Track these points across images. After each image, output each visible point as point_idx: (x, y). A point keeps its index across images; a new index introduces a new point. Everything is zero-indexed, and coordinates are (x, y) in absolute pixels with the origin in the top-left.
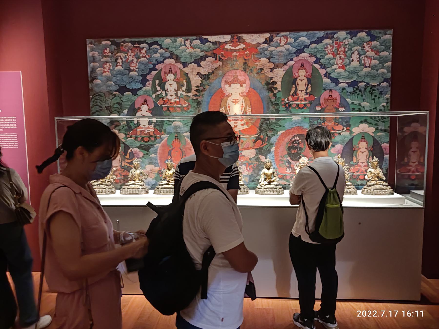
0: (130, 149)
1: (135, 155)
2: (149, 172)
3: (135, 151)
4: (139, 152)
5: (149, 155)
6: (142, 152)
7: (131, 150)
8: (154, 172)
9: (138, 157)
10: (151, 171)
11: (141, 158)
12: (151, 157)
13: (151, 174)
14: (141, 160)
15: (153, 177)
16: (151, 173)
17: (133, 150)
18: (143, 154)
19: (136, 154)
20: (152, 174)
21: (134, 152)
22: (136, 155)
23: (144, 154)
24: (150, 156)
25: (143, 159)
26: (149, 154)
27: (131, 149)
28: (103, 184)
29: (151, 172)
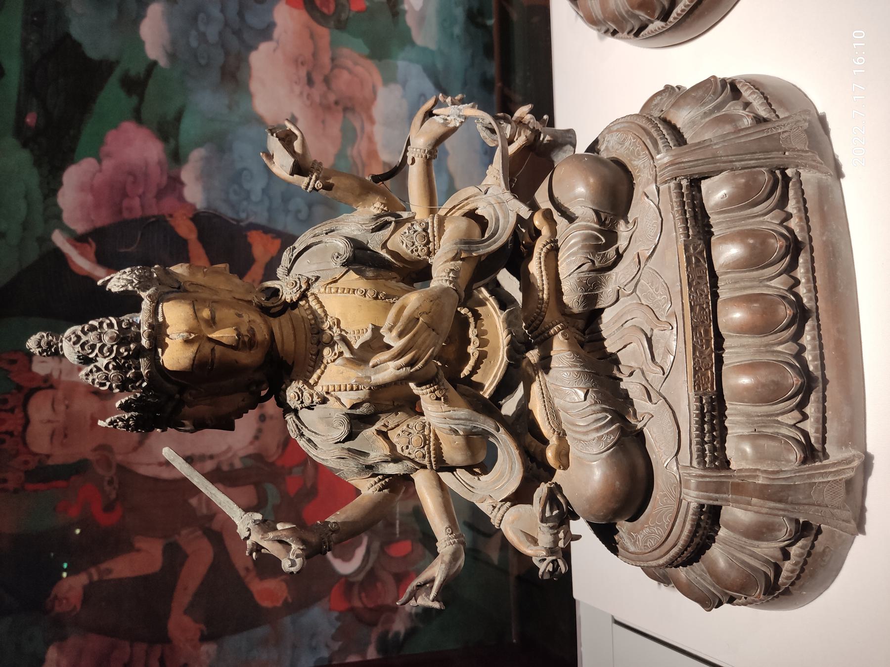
0: (59, 255)
1: (135, 208)
2: (324, 96)
3: (90, 198)
4: (107, 164)
5: (153, 65)
6: (111, 136)
7: (79, 240)
8: (326, 59)
9: (158, 178)
10: (310, 82)
11: (177, 157)
12: (172, 56)
13: (343, 80)
14: (196, 156)
15: (369, 71)
16: (327, 81)
17: (80, 228)
18: (129, 127)
19: (125, 195)
20: (345, 75)
21: (103, 219)
22: (136, 202)
23: (138, 117)
24: (163, 62)
25: (189, 127)
26: (137, 69)
27: (59, 239)
28: (571, 297)
29: (318, 78)
